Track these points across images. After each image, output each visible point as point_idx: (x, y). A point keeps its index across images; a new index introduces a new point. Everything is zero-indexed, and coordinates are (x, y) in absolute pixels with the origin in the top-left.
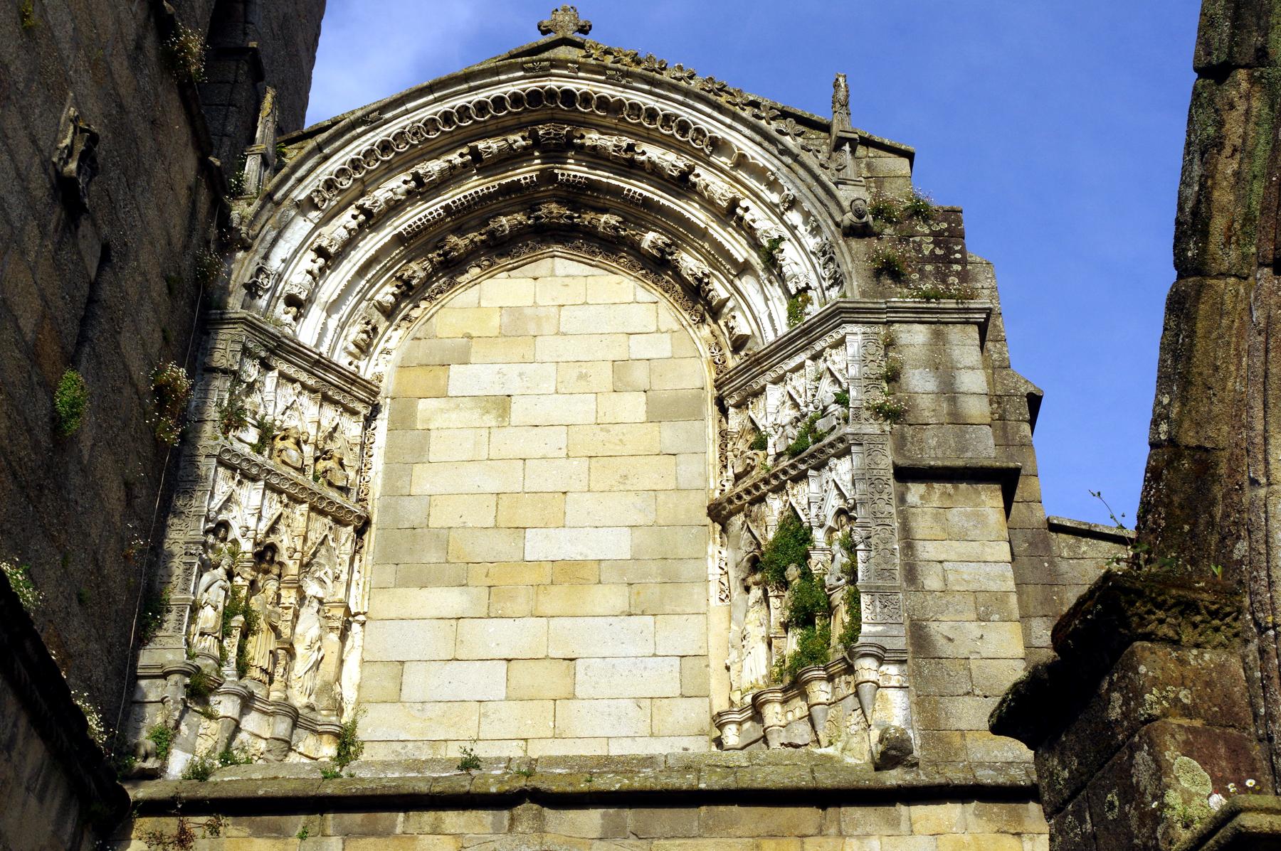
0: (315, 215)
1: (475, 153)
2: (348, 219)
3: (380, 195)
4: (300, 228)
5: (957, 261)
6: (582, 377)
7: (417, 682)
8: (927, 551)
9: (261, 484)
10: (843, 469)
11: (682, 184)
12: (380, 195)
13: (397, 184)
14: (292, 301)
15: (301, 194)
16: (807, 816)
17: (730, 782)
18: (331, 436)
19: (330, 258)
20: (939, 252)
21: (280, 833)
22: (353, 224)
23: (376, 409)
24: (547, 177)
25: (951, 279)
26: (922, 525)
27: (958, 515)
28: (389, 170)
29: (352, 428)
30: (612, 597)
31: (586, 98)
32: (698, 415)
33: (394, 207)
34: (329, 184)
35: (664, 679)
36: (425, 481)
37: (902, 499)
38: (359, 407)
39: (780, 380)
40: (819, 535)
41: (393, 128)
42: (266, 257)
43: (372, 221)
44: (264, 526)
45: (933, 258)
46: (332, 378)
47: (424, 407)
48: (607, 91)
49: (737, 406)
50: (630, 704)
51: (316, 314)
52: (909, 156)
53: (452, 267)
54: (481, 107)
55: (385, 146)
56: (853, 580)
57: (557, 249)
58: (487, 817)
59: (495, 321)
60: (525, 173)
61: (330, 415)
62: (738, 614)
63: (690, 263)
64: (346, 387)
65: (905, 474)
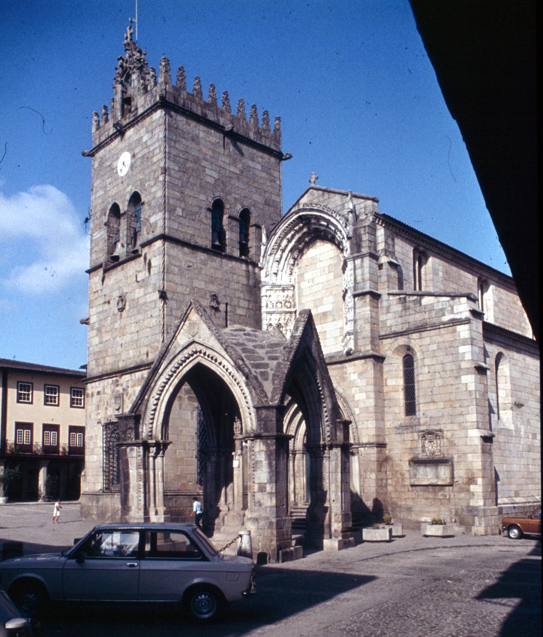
0: (273, 255)
2: (279, 253)
13: (285, 242)
15: (269, 253)
19: (278, 262)
23: (294, 287)
28: (281, 241)
29: (290, 293)
33: (286, 246)
34: (273, 249)
43: (283, 251)
44: (277, 320)
51: (280, 273)
53: (301, 252)
55: (279, 237)
60: (305, 230)
61: (286, 293)
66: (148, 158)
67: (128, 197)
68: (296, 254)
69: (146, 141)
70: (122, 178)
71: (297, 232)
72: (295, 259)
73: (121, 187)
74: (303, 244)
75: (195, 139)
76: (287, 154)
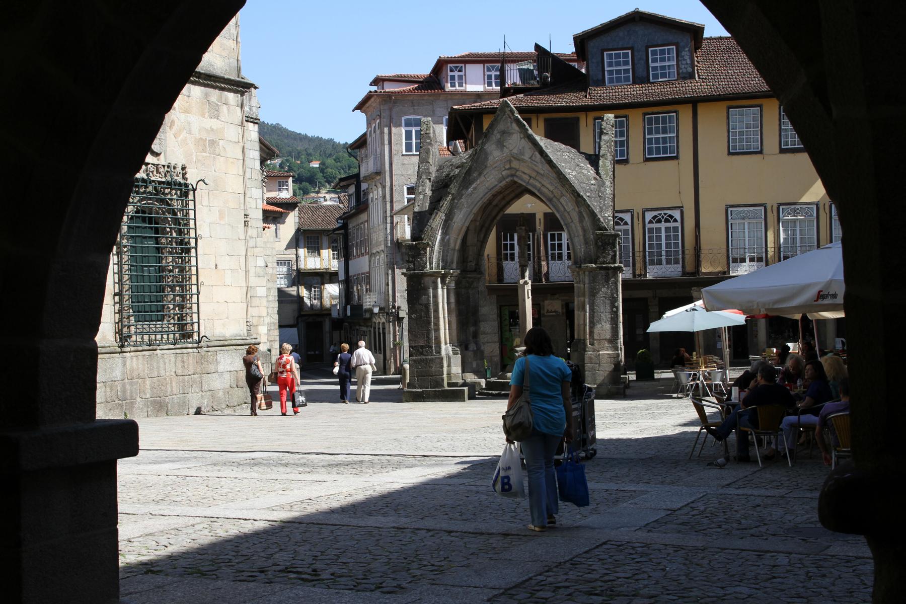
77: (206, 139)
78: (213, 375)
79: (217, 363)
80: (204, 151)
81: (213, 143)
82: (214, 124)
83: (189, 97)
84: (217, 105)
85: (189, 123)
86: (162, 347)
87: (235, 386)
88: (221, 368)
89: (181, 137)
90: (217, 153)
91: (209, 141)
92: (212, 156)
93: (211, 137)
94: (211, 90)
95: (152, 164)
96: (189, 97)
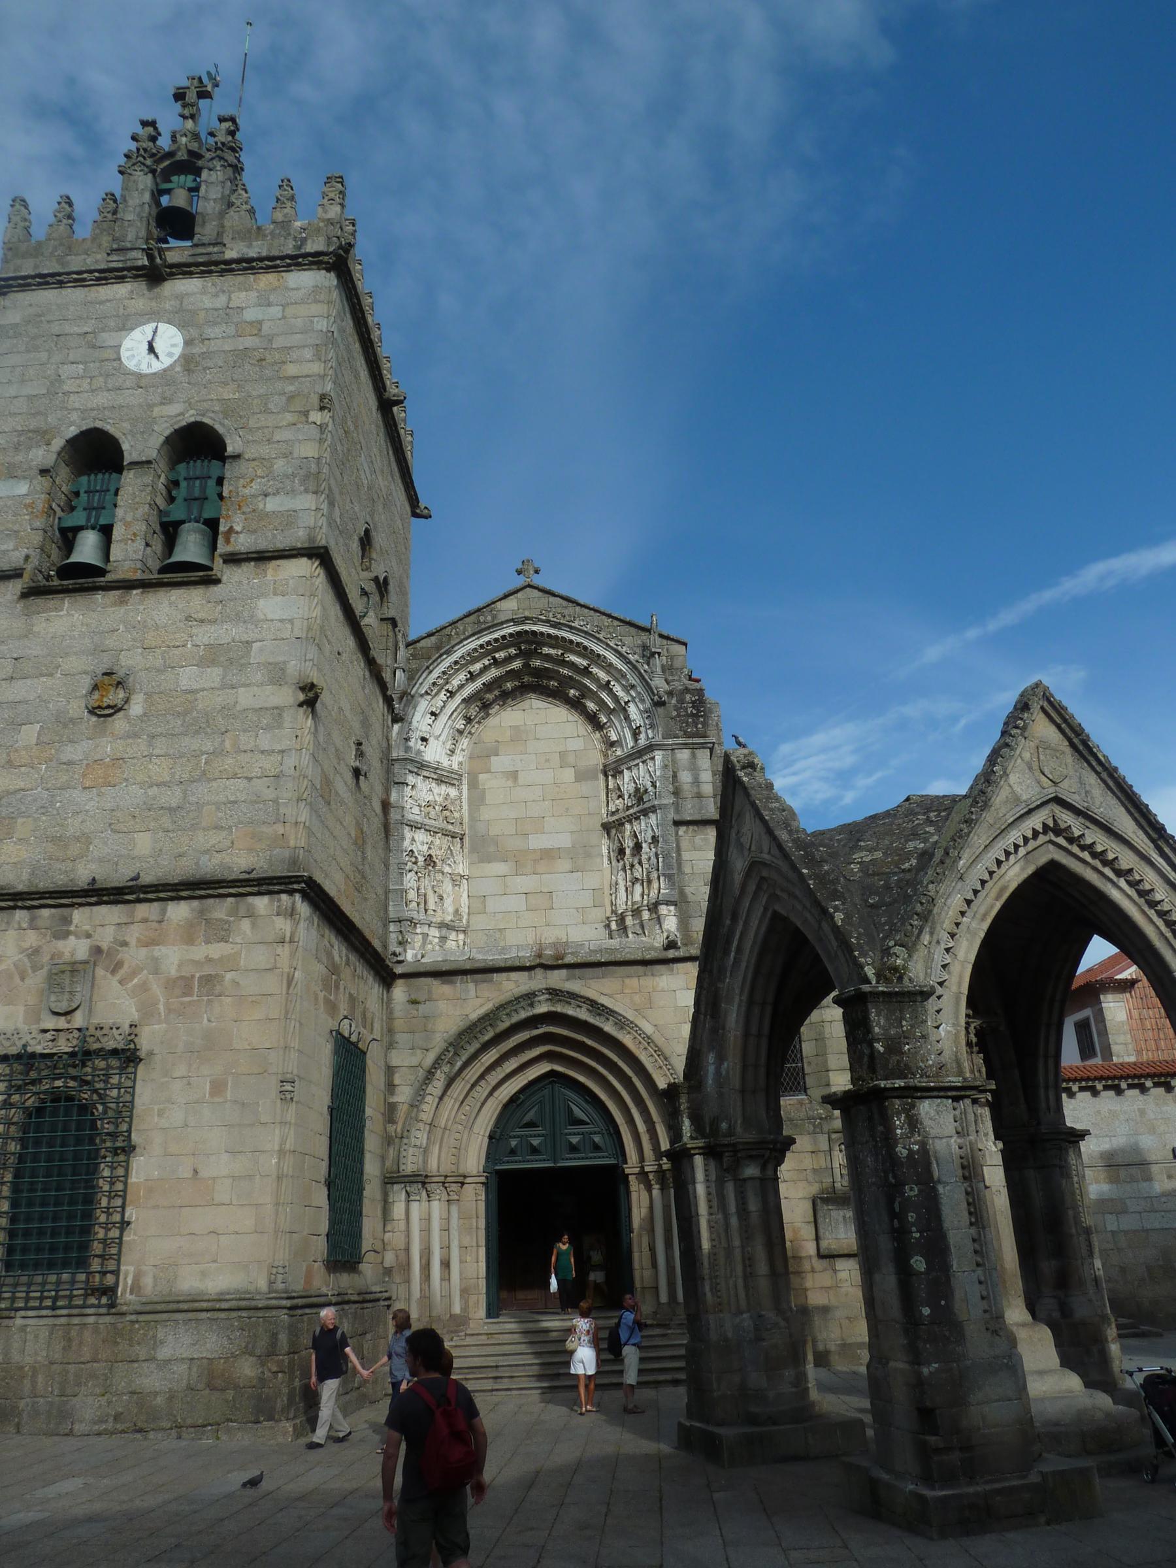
0: (429, 697)
1: (494, 658)
2: (442, 696)
3: (455, 682)
4: (423, 705)
5: (702, 716)
6: (547, 761)
7: (491, 905)
8: (686, 856)
9: (423, 830)
10: (653, 820)
11: (586, 672)
12: (455, 682)
13: (462, 676)
14: (424, 739)
16: (640, 969)
17: (612, 958)
18: (446, 799)
20: (694, 712)
21: (452, 983)
22: (445, 698)
24: (526, 665)
25: (700, 726)
26: (684, 844)
27: (698, 839)
29: (453, 792)
30: (565, 865)
31: (542, 634)
32: (597, 779)
33: (461, 687)
34: (434, 684)
35: (586, 899)
36: (486, 814)
37: (677, 834)
38: (455, 782)
39: (629, 769)
40: (644, 845)
41: (459, 654)
42: (411, 723)
43: (452, 694)
44: (425, 848)
45: (692, 715)
46: (443, 773)
47: (482, 777)
48: (551, 631)
49: (612, 776)
50: (575, 910)
52: (685, 644)
54: (496, 640)
56: (658, 870)
57: (532, 695)
58: (526, 974)
59: (508, 734)
61: (443, 789)
62: (615, 872)
63: (591, 706)
64: (449, 775)
65: (677, 823)
66: (262, 360)
67: (164, 429)
68: (473, 711)
69: (260, 322)
70: (140, 376)
71: (496, 663)
72: (469, 720)
73: (134, 398)
74: (497, 693)
75: (357, 376)
76: (426, 508)
77: (193, 976)
78: (145, 1365)
79: (156, 1343)
80: (185, 994)
81: (208, 981)
82: (216, 950)
83: (160, 922)
84: (227, 922)
85: (155, 960)
86: (22, 1313)
87: (200, 1386)
88: (164, 1353)
89: (136, 980)
90: (216, 992)
91: (200, 977)
92: (206, 998)
93: (208, 970)
94: (211, 901)
95: (54, 1030)
96: (160, 922)
